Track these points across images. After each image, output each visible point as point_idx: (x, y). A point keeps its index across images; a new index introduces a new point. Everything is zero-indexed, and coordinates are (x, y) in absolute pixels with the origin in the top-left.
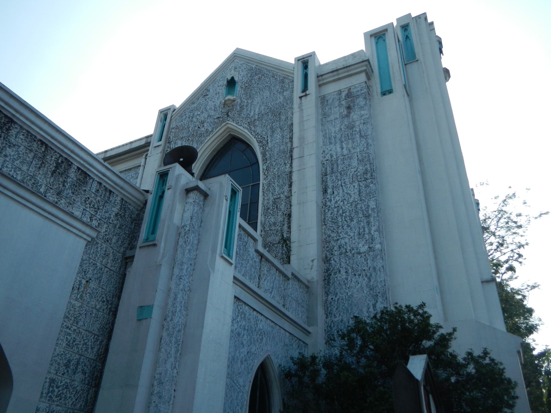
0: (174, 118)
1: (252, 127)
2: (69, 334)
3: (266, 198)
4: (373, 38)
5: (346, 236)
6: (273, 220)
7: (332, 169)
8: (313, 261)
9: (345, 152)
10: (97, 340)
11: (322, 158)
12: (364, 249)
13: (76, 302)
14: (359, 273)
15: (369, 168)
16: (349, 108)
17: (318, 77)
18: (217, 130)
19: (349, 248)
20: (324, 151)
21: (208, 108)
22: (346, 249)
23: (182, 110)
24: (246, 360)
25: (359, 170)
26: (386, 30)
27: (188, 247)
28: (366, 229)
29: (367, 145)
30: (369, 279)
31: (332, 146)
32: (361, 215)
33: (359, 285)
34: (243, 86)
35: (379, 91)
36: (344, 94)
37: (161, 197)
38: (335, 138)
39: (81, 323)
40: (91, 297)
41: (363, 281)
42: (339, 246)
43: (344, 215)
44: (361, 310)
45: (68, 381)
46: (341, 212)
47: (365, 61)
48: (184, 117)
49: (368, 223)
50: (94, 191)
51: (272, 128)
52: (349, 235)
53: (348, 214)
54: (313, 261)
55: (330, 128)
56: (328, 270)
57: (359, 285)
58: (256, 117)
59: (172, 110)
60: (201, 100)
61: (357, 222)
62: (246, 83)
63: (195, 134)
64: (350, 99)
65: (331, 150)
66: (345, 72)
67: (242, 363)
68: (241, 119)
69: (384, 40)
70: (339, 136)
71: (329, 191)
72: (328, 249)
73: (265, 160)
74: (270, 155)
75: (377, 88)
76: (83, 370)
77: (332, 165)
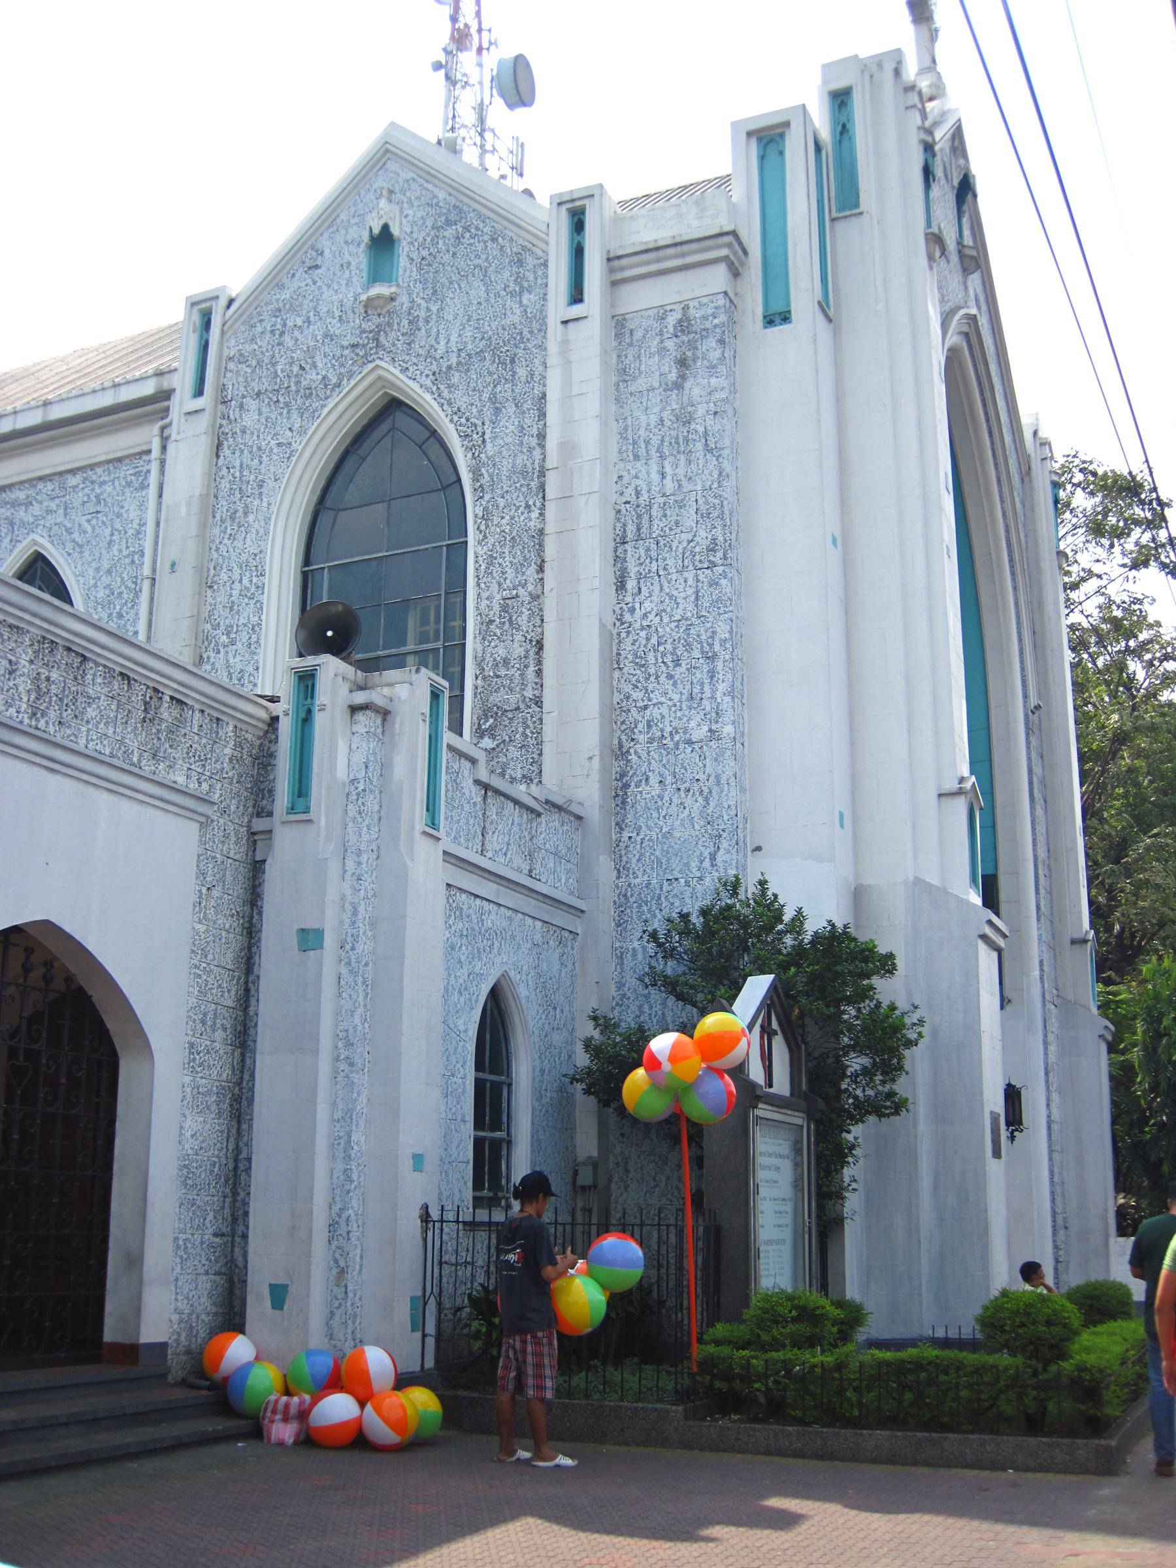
0: (231, 326)
1: (442, 387)
2: (199, 976)
3: (485, 595)
4: (754, 143)
5: (663, 700)
6: (501, 652)
7: (639, 529)
8: (590, 758)
9: (669, 486)
10: (233, 977)
11: (615, 497)
12: (699, 733)
13: (200, 926)
14: (687, 785)
15: (721, 538)
16: (682, 363)
17: (609, 260)
18: (353, 382)
19: (668, 729)
20: (620, 477)
21: (323, 309)
22: (662, 730)
23: (249, 306)
24: (466, 989)
26: (787, 124)
27: (366, 822)
28: (707, 688)
29: (720, 474)
30: (706, 800)
31: (639, 464)
32: (696, 653)
33: (686, 812)
34: (414, 255)
35: (760, 311)
36: (672, 320)
37: (306, 720)
38: (647, 443)
39: (210, 957)
40: (217, 913)
41: (695, 805)
42: (648, 722)
43: (661, 648)
44: (687, 865)
45: (208, 1043)
46: (654, 640)
47: (727, 233)
48: (259, 329)
49: (712, 674)
50: (195, 730)
51: (493, 399)
52: (670, 699)
53: (669, 647)
55: (637, 413)
56: (623, 775)
57: (686, 812)
58: (454, 360)
59: (223, 302)
60: (301, 281)
61: (688, 669)
62: (422, 245)
63: (293, 388)
64: (685, 338)
65: (636, 477)
66: (676, 256)
67: (460, 993)
68: (414, 360)
69: (781, 153)
70: (656, 440)
71: (631, 584)
72: (624, 727)
73: (479, 490)
74: (491, 476)
75: (754, 303)
76: (222, 1025)
77: (639, 517)
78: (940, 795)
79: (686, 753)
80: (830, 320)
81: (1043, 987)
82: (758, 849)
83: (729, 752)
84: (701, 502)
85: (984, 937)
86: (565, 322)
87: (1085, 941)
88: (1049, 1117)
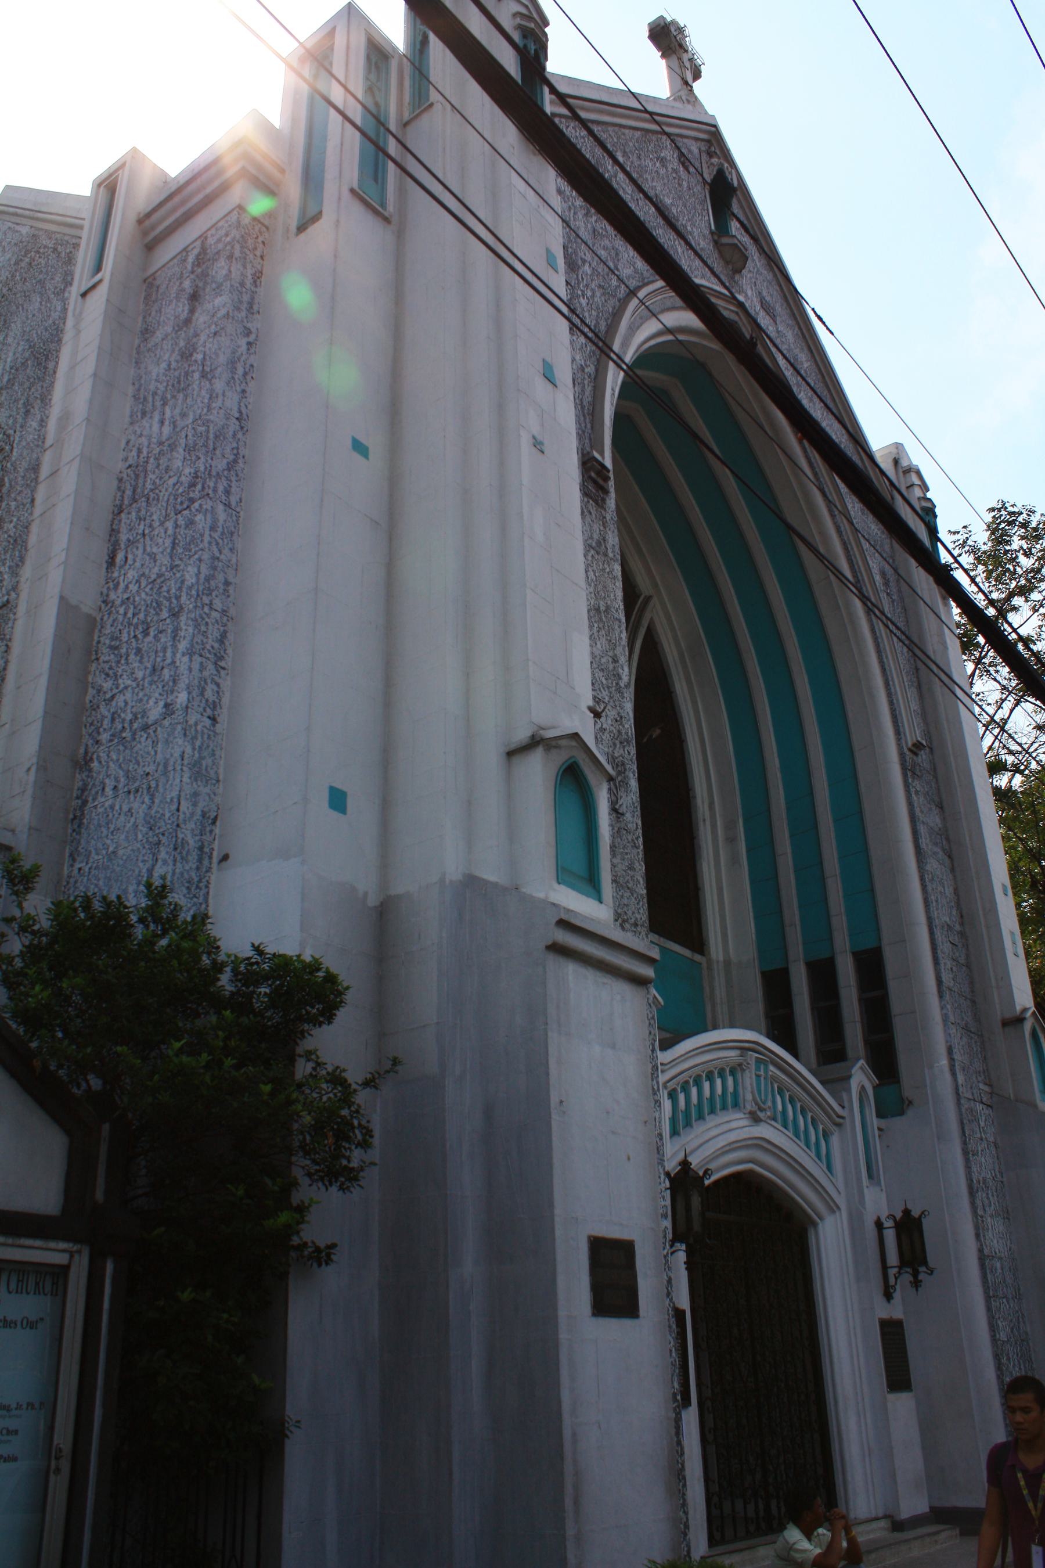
5: (129, 682)
7: (134, 491)
8: (29, 769)
9: (167, 430)
14: (136, 784)
19: (129, 717)
20: (128, 443)
25: (183, 478)
28: (169, 654)
32: (165, 614)
33: (133, 820)
43: (135, 620)
44: (125, 891)
46: (130, 615)
49: (176, 631)
53: (142, 616)
54: (29, 769)
56: (83, 790)
61: (155, 637)
77: (137, 476)
78: (510, 754)
79: (143, 743)
80: (387, 220)
81: (955, 1080)
82: (225, 858)
83: (179, 727)
84: (190, 437)
85: (557, 949)
86: (84, 295)
87: (1020, 1020)
88: (981, 1251)
